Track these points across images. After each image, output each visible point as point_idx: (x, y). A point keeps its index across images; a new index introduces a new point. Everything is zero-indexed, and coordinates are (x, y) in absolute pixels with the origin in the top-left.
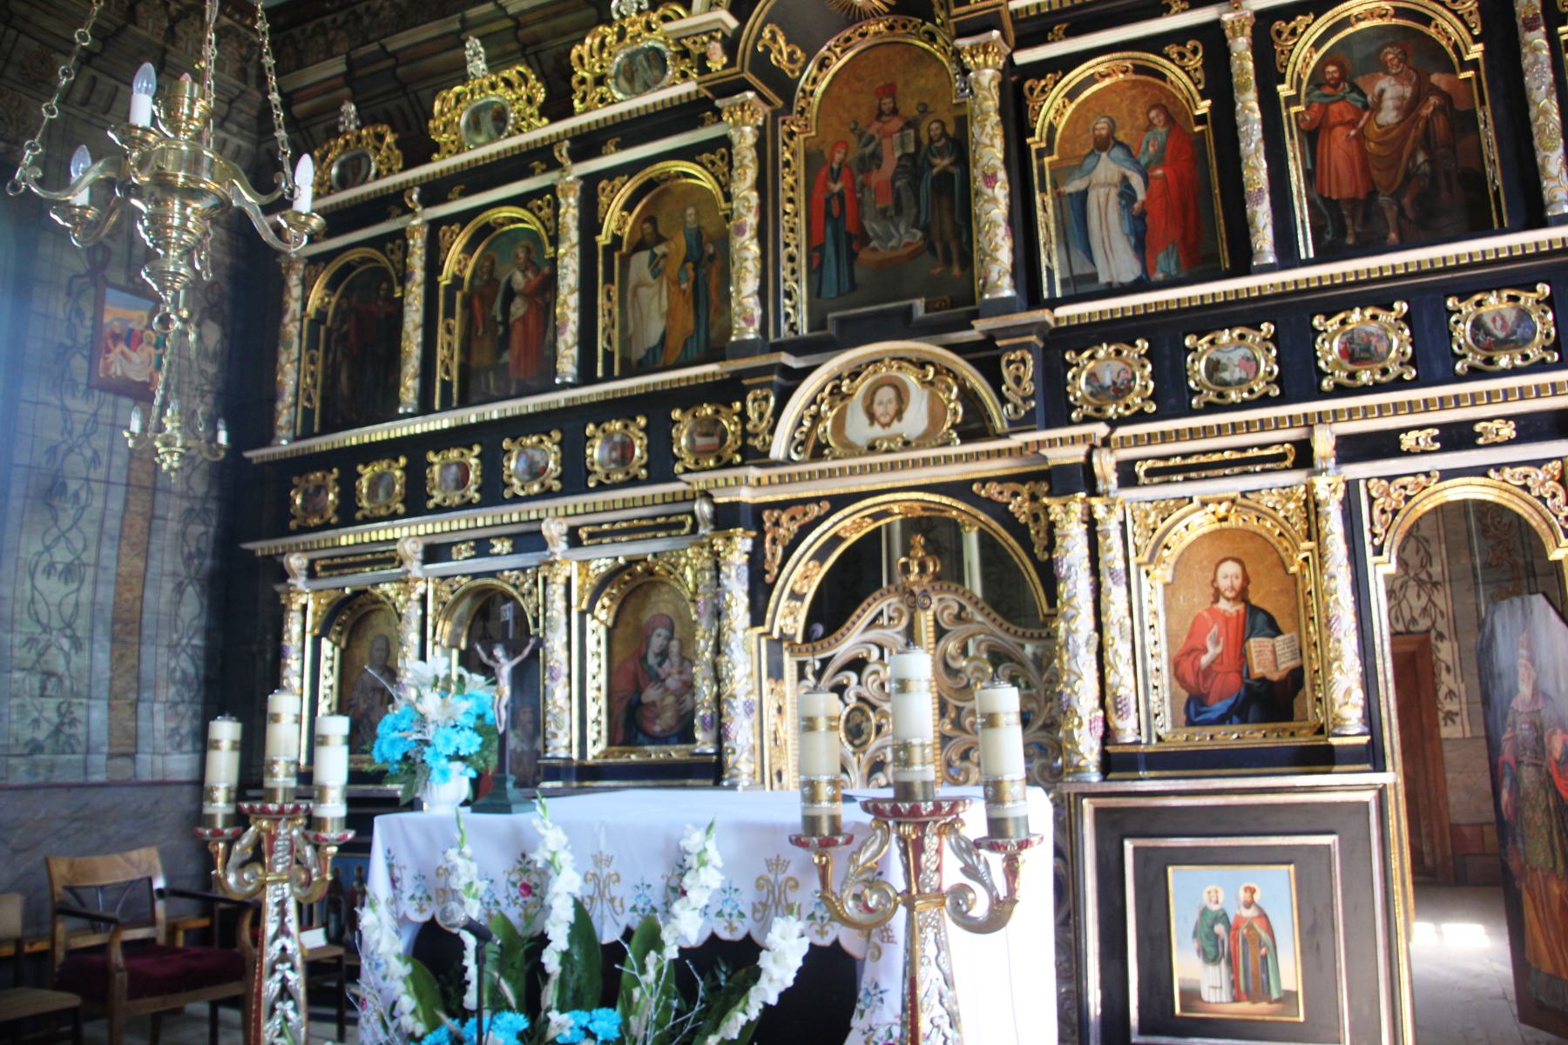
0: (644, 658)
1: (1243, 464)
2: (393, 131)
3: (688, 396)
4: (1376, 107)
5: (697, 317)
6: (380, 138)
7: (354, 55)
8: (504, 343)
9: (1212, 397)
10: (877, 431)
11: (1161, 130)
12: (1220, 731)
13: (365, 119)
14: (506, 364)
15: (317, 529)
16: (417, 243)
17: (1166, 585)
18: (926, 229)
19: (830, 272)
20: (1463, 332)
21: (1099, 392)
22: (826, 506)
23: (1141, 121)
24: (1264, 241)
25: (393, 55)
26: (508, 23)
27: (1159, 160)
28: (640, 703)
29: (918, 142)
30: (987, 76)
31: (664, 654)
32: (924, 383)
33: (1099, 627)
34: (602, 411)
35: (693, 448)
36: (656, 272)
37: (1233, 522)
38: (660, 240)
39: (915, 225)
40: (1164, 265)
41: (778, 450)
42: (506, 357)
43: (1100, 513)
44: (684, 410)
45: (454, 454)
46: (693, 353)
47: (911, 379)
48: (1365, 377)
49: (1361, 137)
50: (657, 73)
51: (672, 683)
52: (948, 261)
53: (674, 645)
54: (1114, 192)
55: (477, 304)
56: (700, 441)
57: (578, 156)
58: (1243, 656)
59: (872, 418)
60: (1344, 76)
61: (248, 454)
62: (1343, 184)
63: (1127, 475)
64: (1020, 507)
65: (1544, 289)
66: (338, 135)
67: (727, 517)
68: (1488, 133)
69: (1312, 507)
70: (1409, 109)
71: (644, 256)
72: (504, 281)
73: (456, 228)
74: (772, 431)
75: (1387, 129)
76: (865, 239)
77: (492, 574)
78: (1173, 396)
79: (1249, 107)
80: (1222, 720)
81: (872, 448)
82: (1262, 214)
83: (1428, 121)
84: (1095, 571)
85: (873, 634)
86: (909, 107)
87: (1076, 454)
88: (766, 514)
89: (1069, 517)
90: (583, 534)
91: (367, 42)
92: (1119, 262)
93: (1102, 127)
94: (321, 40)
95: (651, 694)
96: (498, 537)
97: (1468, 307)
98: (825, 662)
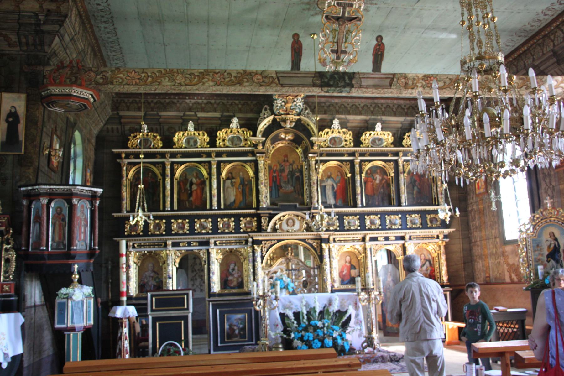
0: (228, 270)
1: (354, 241)
2: (160, 136)
3: (245, 216)
4: (376, 180)
5: (243, 197)
6: (156, 137)
7: (148, 113)
8: (191, 195)
9: (348, 228)
10: (289, 228)
11: (340, 177)
12: (347, 285)
13: (150, 130)
14: (191, 201)
15: (135, 236)
16: (168, 168)
17: (339, 261)
18: (294, 187)
19: (274, 192)
20: (388, 221)
22: (276, 241)
23: (336, 174)
24: (359, 202)
25: (160, 116)
26: (196, 118)
27: (339, 182)
28: (227, 280)
29: (293, 169)
30: (314, 162)
31: (233, 270)
32: (298, 219)
34: (222, 216)
35: (245, 226)
36: (233, 186)
37: (349, 250)
38: (233, 178)
39: (292, 186)
40: (339, 203)
41: (269, 230)
42: (191, 199)
43: (331, 247)
44: (244, 218)
45: (180, 221)
46: (242, 205)
47: (295, 218)
48: (373, 227)
49: (373, 185)
50: (239, 142)
51: (236, 276)
52: (299, 194)
53: (236, 268)
54: (331, 187)
55: (182, 184)
56: (247, 225)
58: (350, 273)
59: (288, 225)
60: (371, 173)
61: (113, 214)
62: (370, 193)
63: (334, 241)
64: (315, 244)
65: (400, 216)
66: (140, 132)
67: (255, 242)
68: (393, 188)
69: (365, 249)
70: (382, 180)
71: (229, 181)
72: (190, 180)
73: (179, 165)
74: (268, 226)
75: (377, 184)
76: (281, 187)
77: (192, 250)
78: (342, 228)
79: (358, 178)
80: (347, 284)
81: (288, 231)
82: (359, 198)
83: (383, 184)
84: (330, 257)
85: (279, 267)
86: (291, 160)
87: (327, 236)
88: (263, 242)
90: (217, 243)
91: (152, 110)
92: (331, 201)
93: (329, 174)
94: (136, 105)
95: (230, 278)
96: (194, 242)
97: (389, 217)
98: (269, 272)
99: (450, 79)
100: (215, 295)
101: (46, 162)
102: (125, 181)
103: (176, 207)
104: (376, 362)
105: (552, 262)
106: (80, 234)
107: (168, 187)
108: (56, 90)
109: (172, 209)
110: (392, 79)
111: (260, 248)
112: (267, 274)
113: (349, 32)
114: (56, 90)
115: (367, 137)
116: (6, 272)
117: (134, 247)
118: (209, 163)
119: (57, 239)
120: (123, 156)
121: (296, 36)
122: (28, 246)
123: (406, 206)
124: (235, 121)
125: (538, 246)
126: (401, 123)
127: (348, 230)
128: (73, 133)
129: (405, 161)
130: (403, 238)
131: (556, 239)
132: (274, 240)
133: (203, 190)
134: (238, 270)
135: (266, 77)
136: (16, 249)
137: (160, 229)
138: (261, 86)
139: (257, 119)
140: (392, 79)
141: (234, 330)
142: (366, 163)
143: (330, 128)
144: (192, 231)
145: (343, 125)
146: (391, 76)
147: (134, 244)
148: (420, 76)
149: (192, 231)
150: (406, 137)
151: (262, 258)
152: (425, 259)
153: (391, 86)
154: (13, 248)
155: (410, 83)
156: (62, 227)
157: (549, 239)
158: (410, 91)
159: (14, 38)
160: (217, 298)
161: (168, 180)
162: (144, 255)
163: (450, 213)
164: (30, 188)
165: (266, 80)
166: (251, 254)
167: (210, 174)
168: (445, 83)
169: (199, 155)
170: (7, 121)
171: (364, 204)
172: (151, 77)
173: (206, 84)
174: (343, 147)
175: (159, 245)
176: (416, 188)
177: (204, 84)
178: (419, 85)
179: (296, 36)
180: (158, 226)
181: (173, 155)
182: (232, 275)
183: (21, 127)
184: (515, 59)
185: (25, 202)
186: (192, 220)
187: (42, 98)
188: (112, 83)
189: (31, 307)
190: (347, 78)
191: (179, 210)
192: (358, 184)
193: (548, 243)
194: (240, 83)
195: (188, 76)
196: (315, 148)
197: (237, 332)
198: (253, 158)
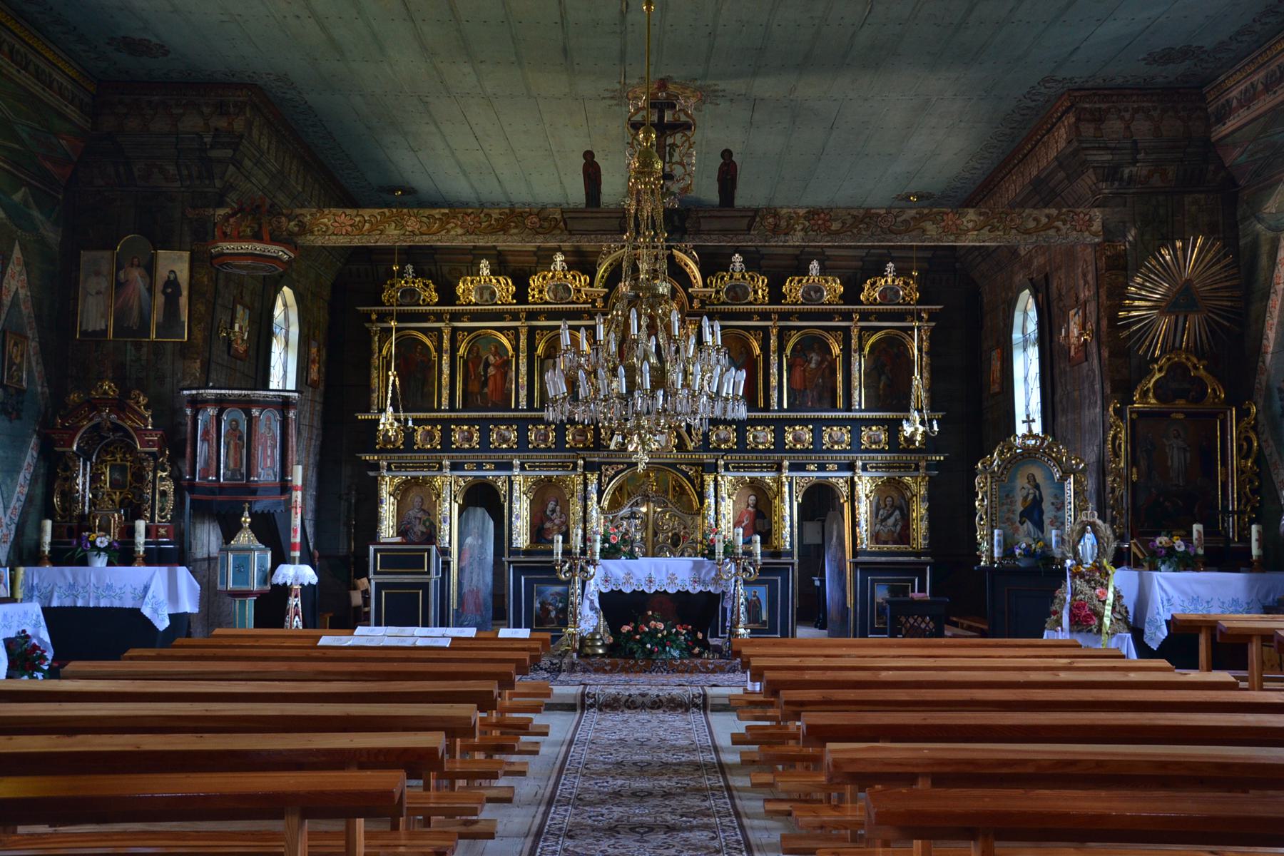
6: (427, 286)
8: (485, 384)
20: (826, 438)
21: (719, 440)
31: (553, 511)
33: (716, 513)
35: (574, 439)
41: (612, 447)
42: (486, 390)
45: (466, 427)
57: (527, 319)
62: (797, 385)
68: (840, 378)
70: (819, 364)
74: (611, 440)
79: (774, 359)
82: (774, 395)
84: (716, 496)
89: (709, 479)
95: (548, 525)
99: (854, 217)
100: (517, 552)
101: (225, 349)
102: (375, 361)
103: (459, 404)
104: (734, 672)
105: (1028, 525)
106: (265, 459)
107: (446, 370)
108: (228, 247)
109: (452, 408)
110: (753, 215)
111: (596, 476)
112: (612, 521)
113: (673, 146)
114: (228, 247)
115: (793, 288)
116: (162, 510)
117: (389, 469)
118: (516, 328)
119: (232, 465)
120: (374, 317)
121: (589, 155)
122: (193, 473)
123: (861, 410)
124: (559, 258)
125: (1007, 496)
126: (862, 259)
127: (754, 450)
128: (278, 290)
129: (862, 328)
130: (851, 467)
131: (1037, 487)
132: (622, 463)
133: (505, 375)
134: (561, 512)
135: (545, 219)
136: (176, 478)
137: (431, 440)
138: (538, 233)
139: (597, 253)
140: (753, 218)
141: (549, 612)
142: (793, 332)
143: (727, 271)
144: (485, 443)
145: (754, 263)
146: (751, 214)
147: (389, 465)
148: (802, 212)
149: (485, 443)
150: (867, 286)
151: (600, 493)
152: (892, 506)
153: (749, 229)
154: (170, 476)
155: (783, 223)
156: (238, 449)
157: (1027, 486)
158: (782, 237)
159: (172, 169)
160: (522, 558)
161: (446, 358)
162: (406, 482)
163: (921, 429)
164: (194, 392)
165: (546, 224)
166: (580, 487)
167: (516, 349)
168: (844, 223)
169: (498, 316)
170: (164, 292)
171: (785, 406)
172: (370, 221)
173: (452, 232)
174: (750, 303)
175: (429, 468)
176: (883, 378)
177: (448, 231)
178: (799, 227)
179: (589, 155)
180: (430, 437)
181: (455, 316)
182: (552, 520)
183: (184, 301)
184: (1020, 161)
185: (189, 411)
186: (485, 425)
187: (213, 257)
188: (312, 232)
189: (204, 559)
190: (676, 218)
191: (465, 409)
192: (774, 370)
193: (1025, 492)
194: (504, 229)
195: (424, 219)
196: (696, 304)
197: (553, 614)
198: (592, 323)
